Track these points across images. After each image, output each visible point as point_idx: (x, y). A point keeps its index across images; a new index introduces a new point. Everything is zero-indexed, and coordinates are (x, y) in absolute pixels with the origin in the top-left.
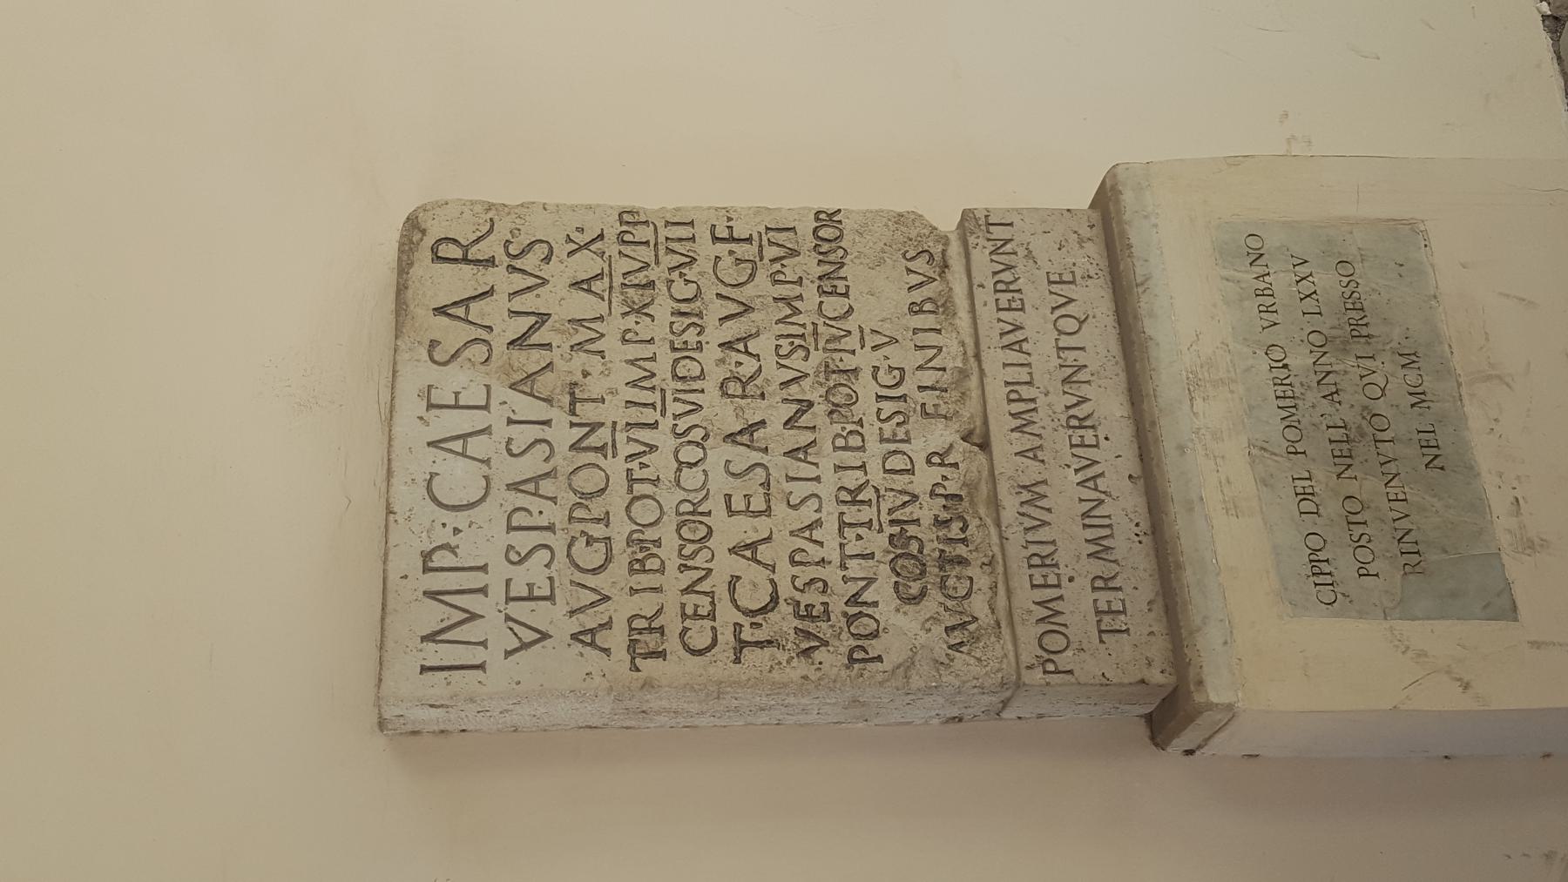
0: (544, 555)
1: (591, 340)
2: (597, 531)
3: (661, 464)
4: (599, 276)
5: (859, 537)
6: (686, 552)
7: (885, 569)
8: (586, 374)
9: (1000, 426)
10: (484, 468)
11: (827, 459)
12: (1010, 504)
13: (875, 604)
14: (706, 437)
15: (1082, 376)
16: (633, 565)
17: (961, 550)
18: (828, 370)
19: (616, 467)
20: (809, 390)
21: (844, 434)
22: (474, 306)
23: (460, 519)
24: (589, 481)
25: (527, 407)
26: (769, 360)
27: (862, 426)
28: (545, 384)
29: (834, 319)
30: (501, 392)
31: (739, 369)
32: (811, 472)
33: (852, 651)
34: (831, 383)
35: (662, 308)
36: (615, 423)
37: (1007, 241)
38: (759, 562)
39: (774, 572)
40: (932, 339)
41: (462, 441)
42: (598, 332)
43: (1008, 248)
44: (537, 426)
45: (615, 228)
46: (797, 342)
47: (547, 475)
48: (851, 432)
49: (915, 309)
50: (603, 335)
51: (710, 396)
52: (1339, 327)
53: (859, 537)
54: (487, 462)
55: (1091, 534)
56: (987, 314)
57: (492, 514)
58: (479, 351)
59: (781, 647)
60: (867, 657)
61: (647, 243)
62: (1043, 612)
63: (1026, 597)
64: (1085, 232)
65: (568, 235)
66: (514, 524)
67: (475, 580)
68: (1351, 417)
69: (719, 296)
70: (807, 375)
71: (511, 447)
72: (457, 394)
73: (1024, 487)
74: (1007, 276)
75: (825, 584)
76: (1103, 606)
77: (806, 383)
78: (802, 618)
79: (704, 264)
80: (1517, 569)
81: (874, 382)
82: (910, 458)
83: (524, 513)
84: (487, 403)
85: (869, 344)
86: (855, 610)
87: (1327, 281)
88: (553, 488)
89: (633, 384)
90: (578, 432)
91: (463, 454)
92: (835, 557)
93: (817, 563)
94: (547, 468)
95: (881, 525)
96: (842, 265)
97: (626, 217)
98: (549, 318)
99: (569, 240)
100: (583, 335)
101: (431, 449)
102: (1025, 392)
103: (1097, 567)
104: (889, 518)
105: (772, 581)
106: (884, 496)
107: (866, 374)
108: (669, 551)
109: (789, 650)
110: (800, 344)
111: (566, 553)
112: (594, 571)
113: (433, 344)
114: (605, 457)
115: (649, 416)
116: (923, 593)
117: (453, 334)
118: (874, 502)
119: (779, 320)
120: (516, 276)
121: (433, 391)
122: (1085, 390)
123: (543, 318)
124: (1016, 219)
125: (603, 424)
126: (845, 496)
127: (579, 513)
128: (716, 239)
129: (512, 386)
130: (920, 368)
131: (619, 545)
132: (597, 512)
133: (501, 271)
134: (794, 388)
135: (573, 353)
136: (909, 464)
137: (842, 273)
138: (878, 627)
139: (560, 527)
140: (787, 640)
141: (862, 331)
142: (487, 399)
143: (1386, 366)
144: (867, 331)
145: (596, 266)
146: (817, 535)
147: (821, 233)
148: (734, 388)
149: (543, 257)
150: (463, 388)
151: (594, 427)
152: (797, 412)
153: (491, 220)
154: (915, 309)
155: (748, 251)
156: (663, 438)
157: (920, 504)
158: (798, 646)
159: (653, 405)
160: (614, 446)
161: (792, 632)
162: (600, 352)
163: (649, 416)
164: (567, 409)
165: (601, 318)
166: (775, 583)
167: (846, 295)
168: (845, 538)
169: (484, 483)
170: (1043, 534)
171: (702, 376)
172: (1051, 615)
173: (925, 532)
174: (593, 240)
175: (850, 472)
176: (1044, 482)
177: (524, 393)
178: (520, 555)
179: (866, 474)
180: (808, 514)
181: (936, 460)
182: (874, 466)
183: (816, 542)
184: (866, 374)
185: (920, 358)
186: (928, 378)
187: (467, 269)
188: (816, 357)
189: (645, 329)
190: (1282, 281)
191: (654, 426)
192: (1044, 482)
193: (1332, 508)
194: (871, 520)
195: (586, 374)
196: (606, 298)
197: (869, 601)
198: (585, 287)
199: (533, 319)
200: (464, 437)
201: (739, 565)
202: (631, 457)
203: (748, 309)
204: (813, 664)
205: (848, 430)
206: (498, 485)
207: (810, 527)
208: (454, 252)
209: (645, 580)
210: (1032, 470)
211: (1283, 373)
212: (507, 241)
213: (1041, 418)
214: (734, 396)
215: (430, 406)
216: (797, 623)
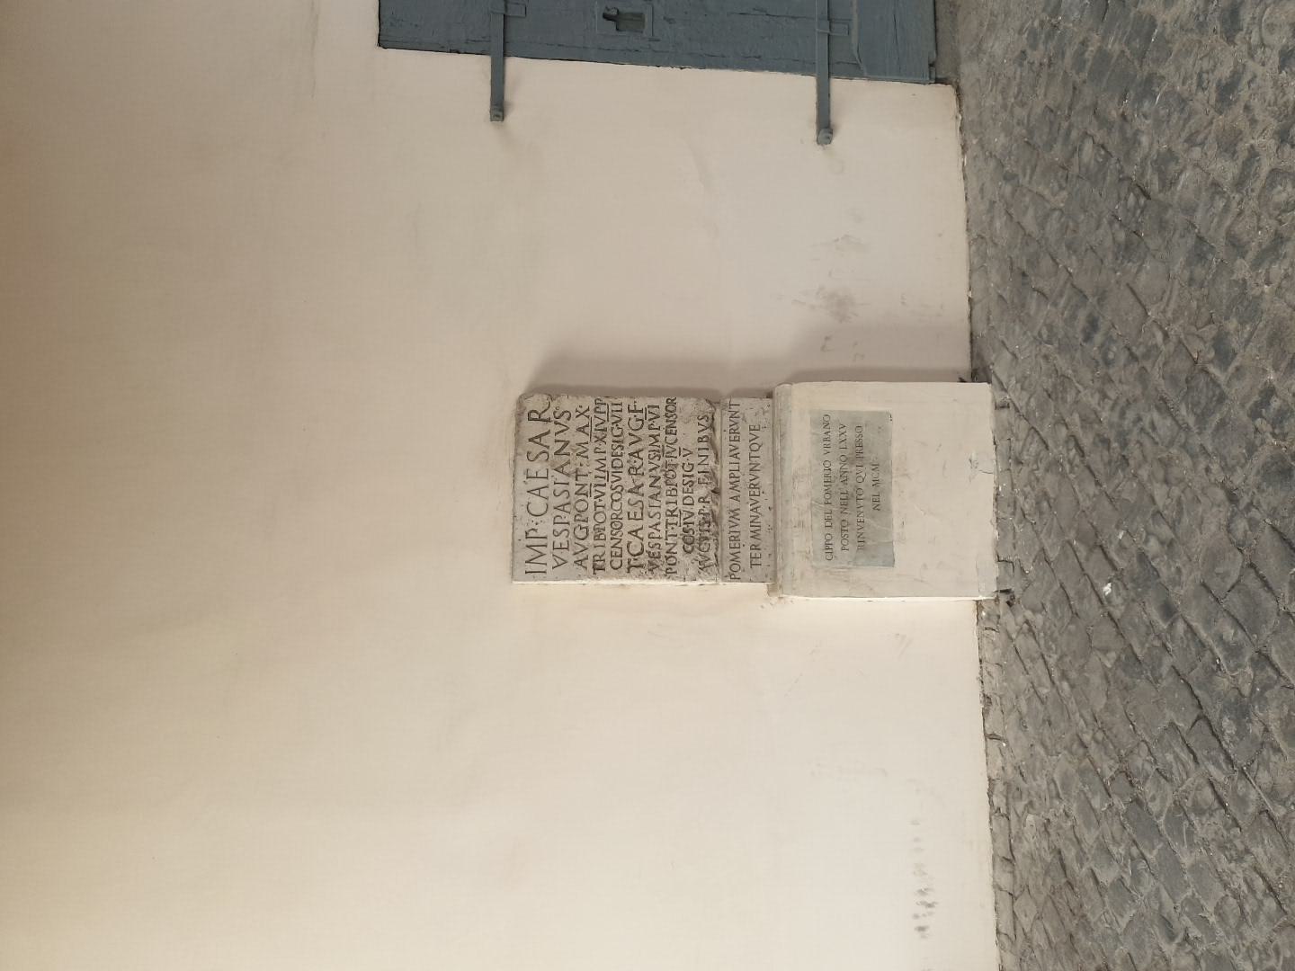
0: (566, 532)
1: (585, 452)
2: (584, 525)
3: (606, 500)
4: (587, 426)
5: (673, 528)
6: (614, 532)
7: (680, 541)
8: (581, 465)
9: (725, 486)
11: (664, 499)
12: (726, 517)
14: (622, 490)
15: (757, 468)
17: (707, 534)
18: (667, 465)
19: (591, 500)
20: (658, 473)
22: (543, 438)
23: (539, 518)
24: (581, 506)
25: (561, 478)
26: (646, 461)
28: (566, 469)
29: (671, 444)
30: (552, 472)
35: (609, 439)
37: (736, 412)
40: (705, 452)
43: (736, 415)
45: (592, 407)
49: (700, 440)
51: (624, 475)
52: (852, 454)
54: (547, 498)
55: (753, 529)
56: (726, 442)
57: (549, 518)
58: (545, 455)
61: (604, 413)
62: (733, 557)
63: (728, 551)
64: (766, 408)
67: (543, 542)
68: (850, 490)
69: (630, 434)
73: (732, 511)
74: (734, 427)
76: (753, 555)
77: (658, 470)
79: (625, 421)
80: (897, 549)
85: (682, 454)
87: (851, 435)
89: (597, 469)
92: (664, 536)
94: (567, 501)
96: (675, 422)
97: (598, 402)
100: (581, 450)
102: (736, 474)
103: (753, 541)
107: (680, 468)
108: (608, 532)
110: (659, 453)
112: (583, 539)
113: (529, 453)
115: (603, 482)
116: (693, 549)
117: (536, 449)
122: (758, 474)
123: (567, 443)
126: (669, 513)
127: (577, 518)
128: (629, 411)
129: (556, 470)
131: (591, 530)
133: (552, 424)
143: (868, 468)
145: (586, 421)
146: (658, 527)
147: (668, 408)
148: (632, 471)
151: (583, 486)
154: (700, 440)
155: (640, 416)
156: (606, 490)
159: (604, 478)
163: (603, 482)
170: (737, 529)
171: (622, 467)
172: (735, 559)
173: (695, 527)
176: (739, 509)
180: (655, 520)
182: (680, 502)
184: (680, 468)
186: (701, 468)
188: (663, 460)
189: (603, 447)
190: (834, 435)
191: (605, 485)
192: (739, 509)
193: (837, 524)
200: (539, 489)
201: (631, 538)
202: (596, 498)
203: (640, 440)
206: (551, 509)
207: (656, 525)
208: (535, 416)
209: (599, 543)
210: (735, 505)
211: (827, 472)
213: (741, 484)
216: (649, 559)
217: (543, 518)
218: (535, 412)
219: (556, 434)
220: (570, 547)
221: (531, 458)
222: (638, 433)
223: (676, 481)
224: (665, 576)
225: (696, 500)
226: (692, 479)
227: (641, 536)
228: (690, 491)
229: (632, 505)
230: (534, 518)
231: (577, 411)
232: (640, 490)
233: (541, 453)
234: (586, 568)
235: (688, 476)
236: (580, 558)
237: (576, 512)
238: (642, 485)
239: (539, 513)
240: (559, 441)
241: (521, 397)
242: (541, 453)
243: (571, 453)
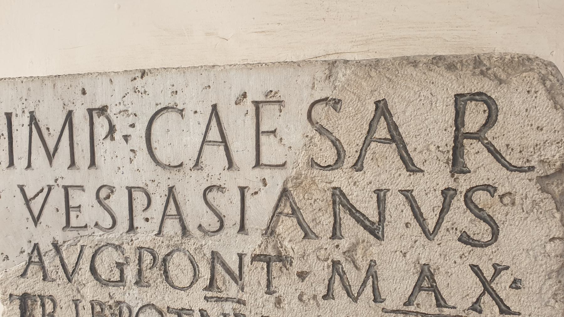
0: (108, 222)
2: (131, 273)
10: (192, 164)
16: (100, 305)
22: (391, 150)
23: (139, 141)
36: (244, 303)
41: (221, 140)
42: (359, 294)
44: (238, 219)
47: (185, 230)
50: (355, 300)
65: (507, 268)
66: (135, 194)
67: (83, 158)
71: (215, 189)
72: (274, 132)
83: (146, 202)
84: (266, 165)
88: (172, 233)
90: (234, 265)
91: (204, 141)
94: (192, 226)
98: (378, 238)
99: (498, 269)
101: (211, 108)
111: (109, 242)
112: (93, 270)
113: (336, 103)
114: (205, 289)
120: (438, 201)
121: (277, 107)
125: (243, 291)
127: (147, 258)
129: (285, 192)
131: (118, 293)
132: (150, 274)
135: (329, 262)
139: (134, 239)
142: (270, 166)
149: (470, 233)
150: (281, 139)
151: (238, 278)
153: (531, 168)
160: (219, 299)
162: (333, 295)
164: (258, 252)
165: (377, 298)
169: (176, 164)
174: (501, 300)
177: (277, 206)
178: (105, 199)
187: (449, 139)
195: (302, 275)
196: (412, 308)
198: (425, 284)
199: (376, 219)
206: (174, 178)
212: (495, 189)
215: (257, 104)
217: (143, 155)
218: (490, 121)
219: (407, 194)
220: (71, 234)
221: (320, 112)
230: (141, 129)
231: (498, 269)
233: (336, 143)
234: (24, 275)
236: (47, 261)
237: (162, 253)
239: (154, 145)
240: (381, 202)
241: (550, 64)
242: (336, 143)
243: (345, 244)
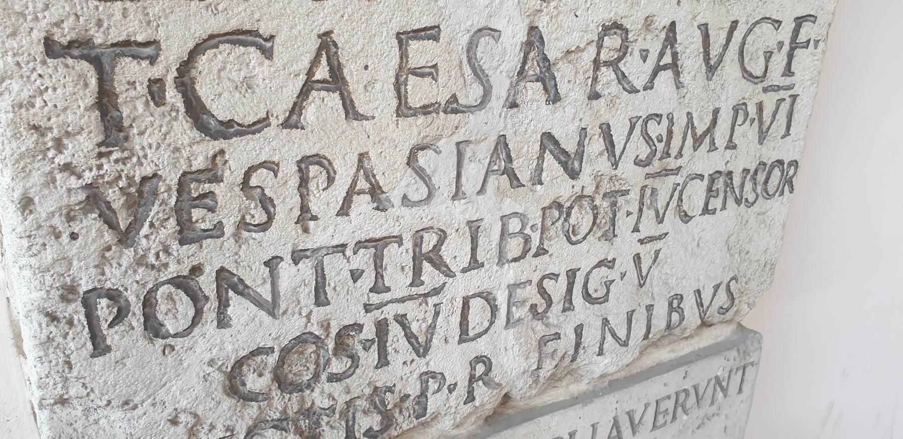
5: (356, 275)
7: (293, 327)
13: (223, 322)
21: (528, 231)
26: (642, 104)
27: (536, 255)
31: (637, 53)
32: (470, 182)
33: (113, 296)
34: (597, 202)
38: (304, 93)
39: (287, 124)
46: (660, 146)
48: (527, 240)
53: (356, 275)
59: (103, 149)
60: (104, 326)
70: (615, 165)
75: (264, 227)
77: (603, 165)
78: (182, 186)
81: (596, 261)
82: (486, 331)
86: (207, 283)
93: (304, 208)
95: (380, 306)
104: (390, 318)
105: (262, 123)
106: (427, 304)
109: (100, 167)
118: (415, 290)
119: (692, 118)
124: (743, 396)
126: (430, 241)
130: (606, 322)
134: (596, 145)
136: (477, 331)
137: (731, 203)
138: (176, 335)
140: (124, 161)
141: (660, 238)
144: (658, 245)
146: (362, 204)
152: (564, 152)
154: (675, 304)
157: (413, 361)
158: (110, 184)
161: (148, 170)
166: (259, 131)
167: (706, 211)
168: (355, 253)
175: (468, 248)
179: (464, 271)
181: (480, 369)
182: (475, 281)
183: (347, 202)
185: (619, 325)
186: (591, 337)
194: (388, 289)
197: (230, 311)
204: (70, 218)
205: (533, 235)
207: (375, 191)
214: (600, 47)
216: (172, 179)
222: (730, 69)
223: (558, 245)
224: (68, 292)
225: (481, 346)
226: (557, 308)
227: (310, 113)
228: (517, 313)
229: (471, 47)
232: (533, 91)
235: (570, 290)
238: (554, 98)
